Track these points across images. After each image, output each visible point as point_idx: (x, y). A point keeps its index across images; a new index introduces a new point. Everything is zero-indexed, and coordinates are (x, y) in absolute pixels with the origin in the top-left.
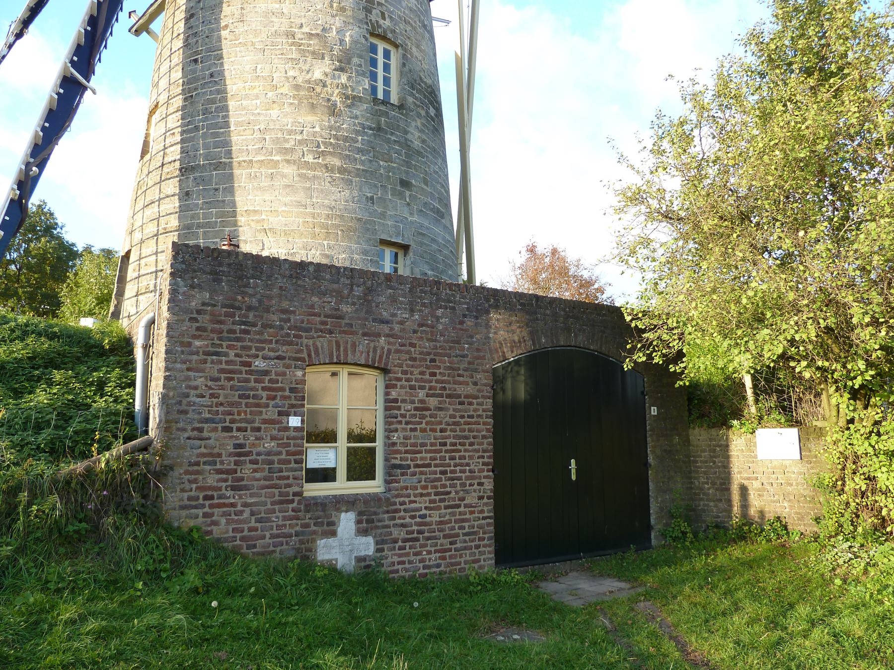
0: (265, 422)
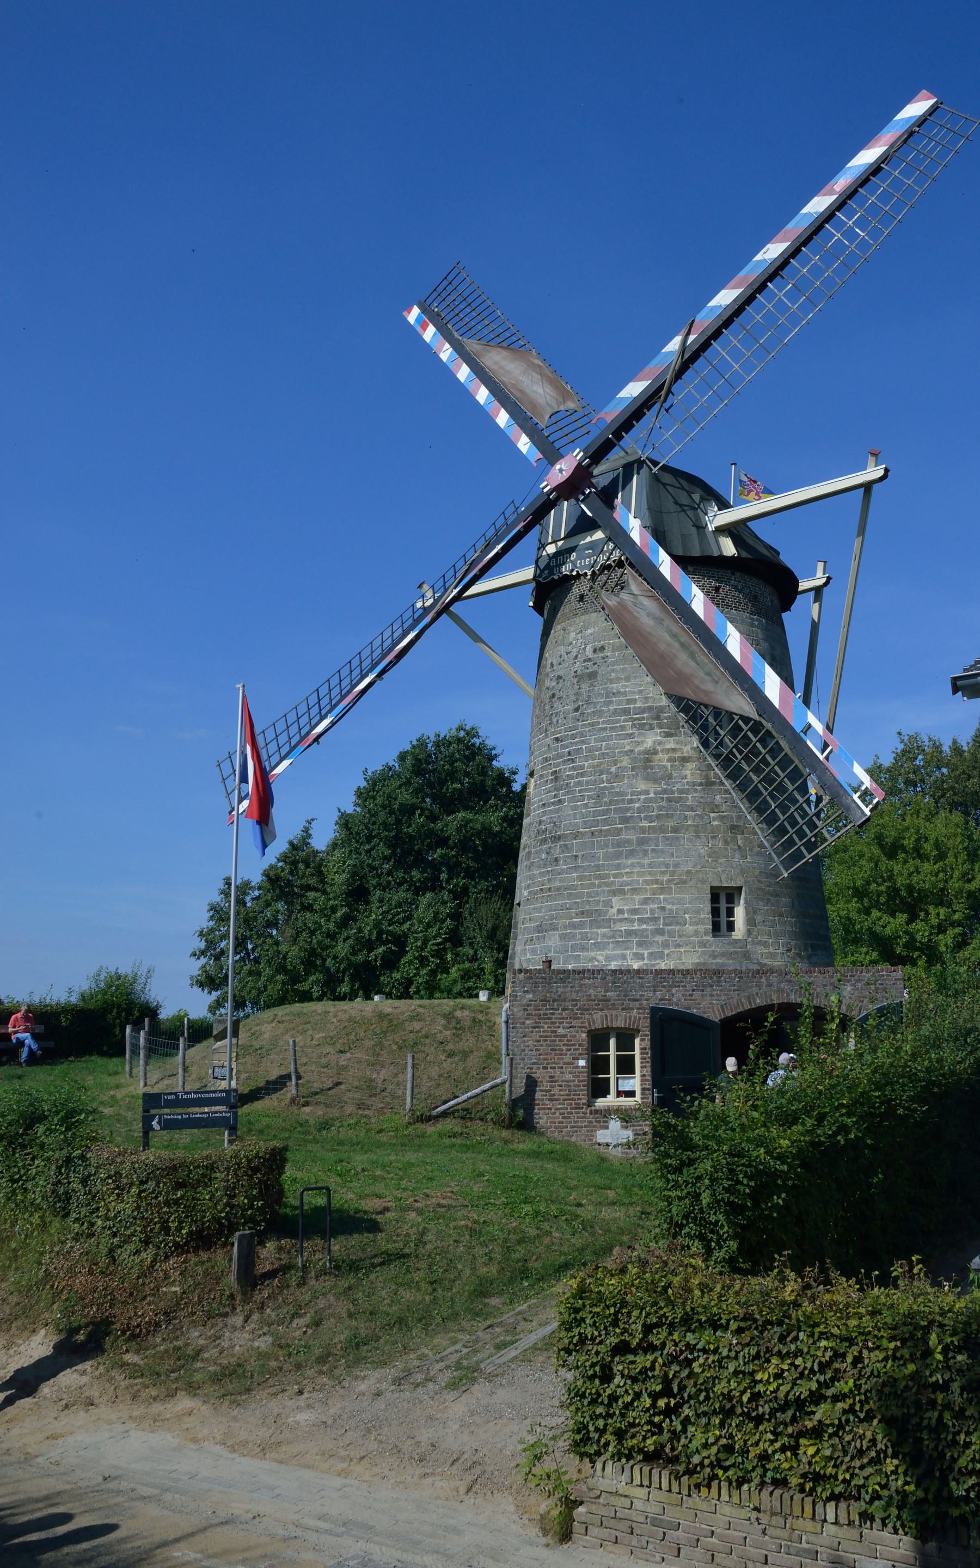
0: (565, 1063)
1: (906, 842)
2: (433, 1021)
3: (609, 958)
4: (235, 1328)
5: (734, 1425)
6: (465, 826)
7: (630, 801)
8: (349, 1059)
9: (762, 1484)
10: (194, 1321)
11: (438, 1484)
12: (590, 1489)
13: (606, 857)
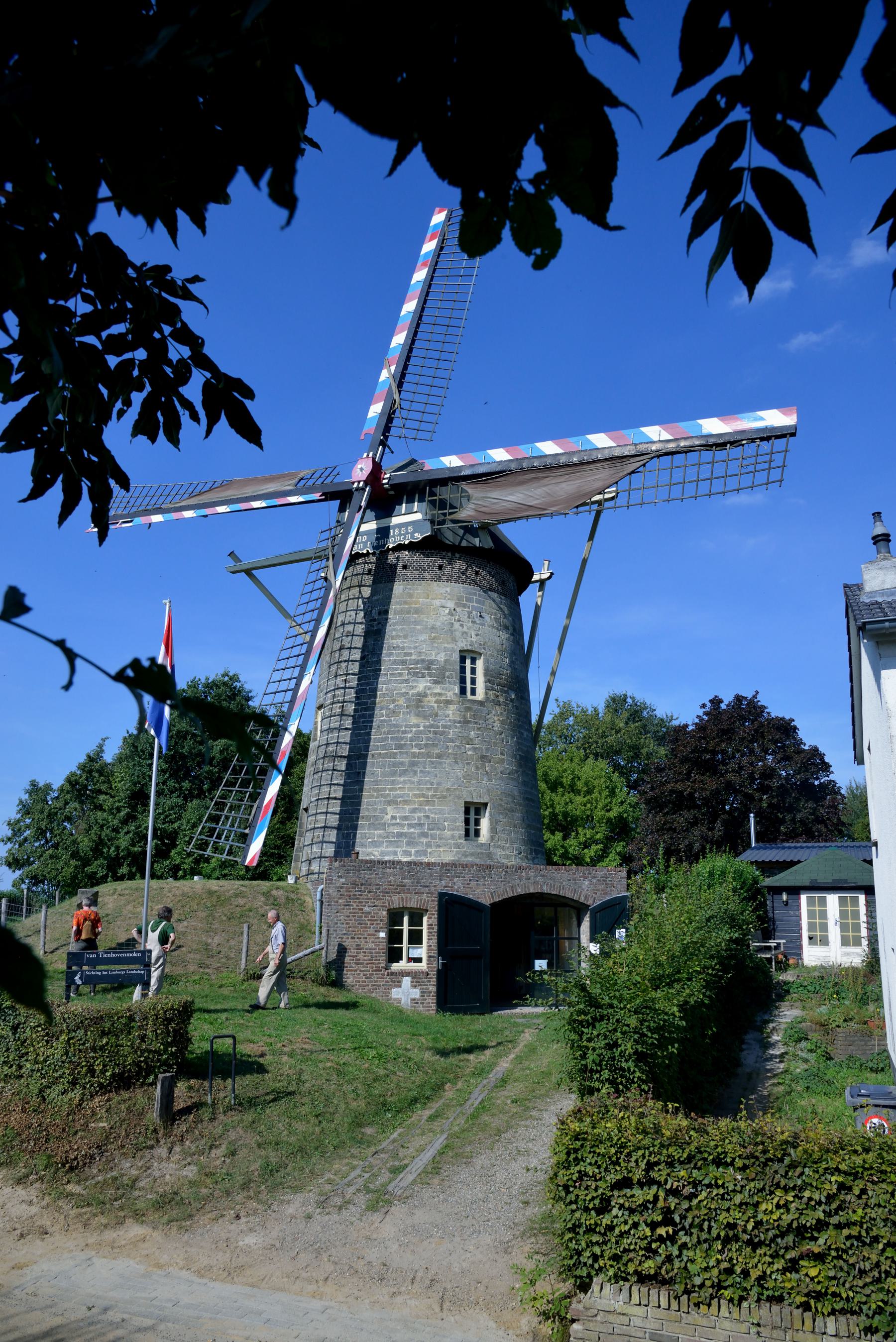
1: (564, 780)
2: (254, 897)
3: (382, 853)
4: (161, 1159)
5: (734, 1250)
6: (227, 749)
7: (405, 732)
8: (187, 927)
9: (759, 1300)
10: (124, 1154)
11: (412, 1303)
12: (587, 1309)
13: (384, 775)
